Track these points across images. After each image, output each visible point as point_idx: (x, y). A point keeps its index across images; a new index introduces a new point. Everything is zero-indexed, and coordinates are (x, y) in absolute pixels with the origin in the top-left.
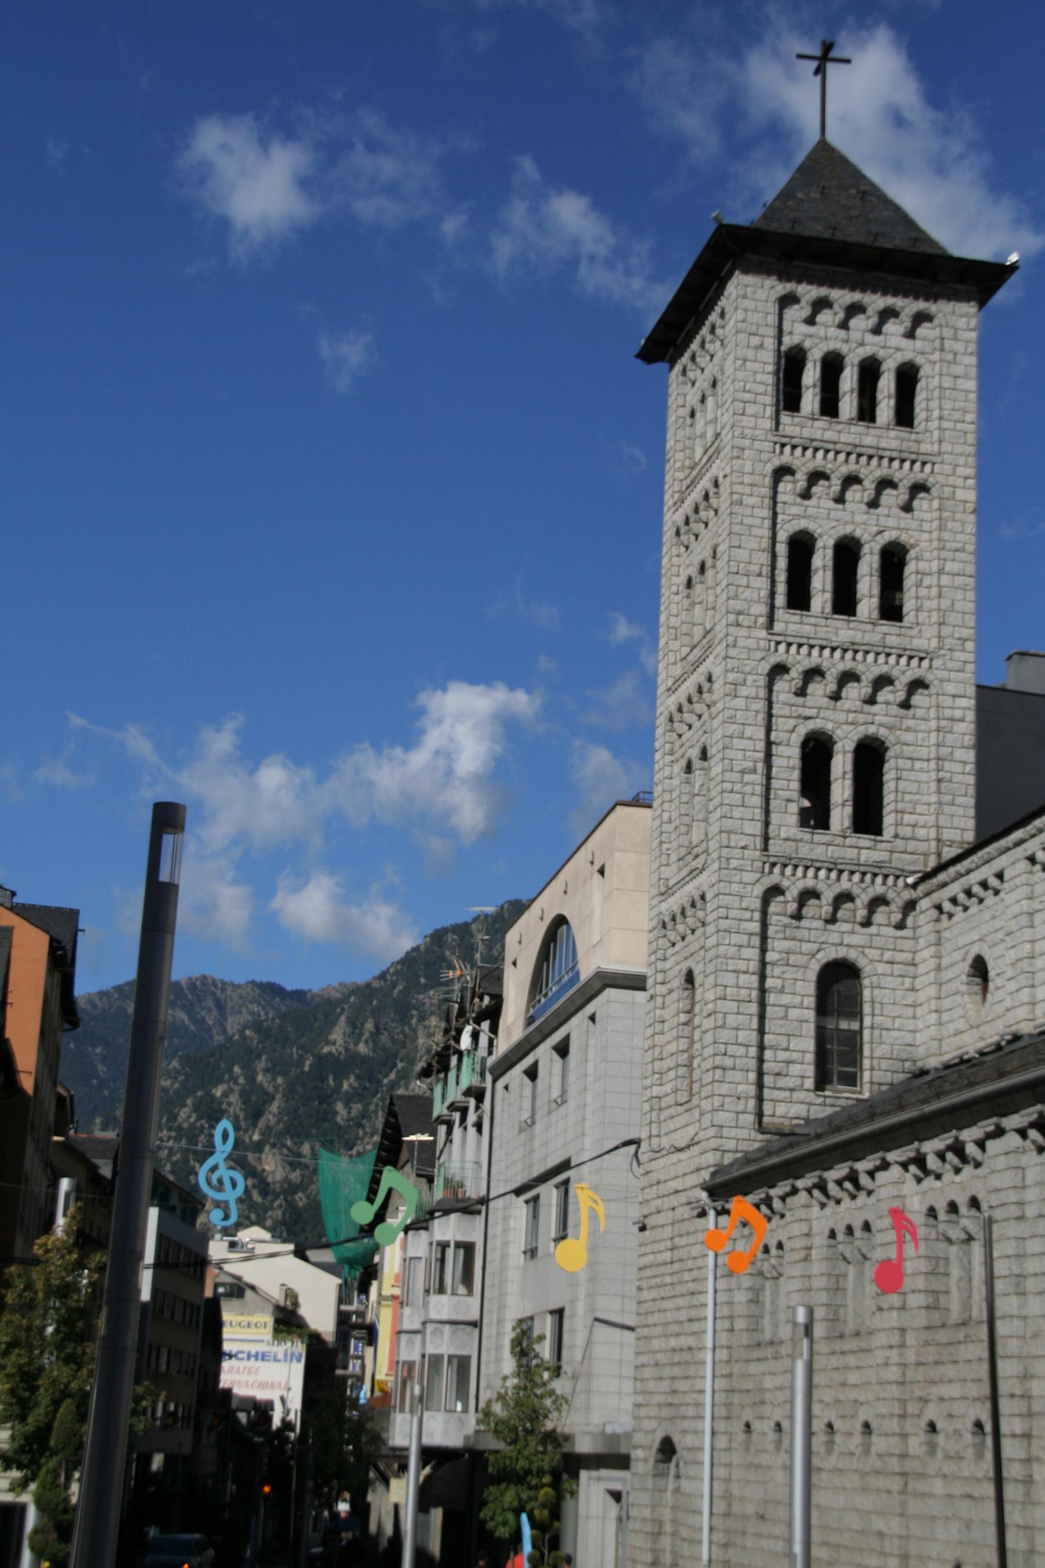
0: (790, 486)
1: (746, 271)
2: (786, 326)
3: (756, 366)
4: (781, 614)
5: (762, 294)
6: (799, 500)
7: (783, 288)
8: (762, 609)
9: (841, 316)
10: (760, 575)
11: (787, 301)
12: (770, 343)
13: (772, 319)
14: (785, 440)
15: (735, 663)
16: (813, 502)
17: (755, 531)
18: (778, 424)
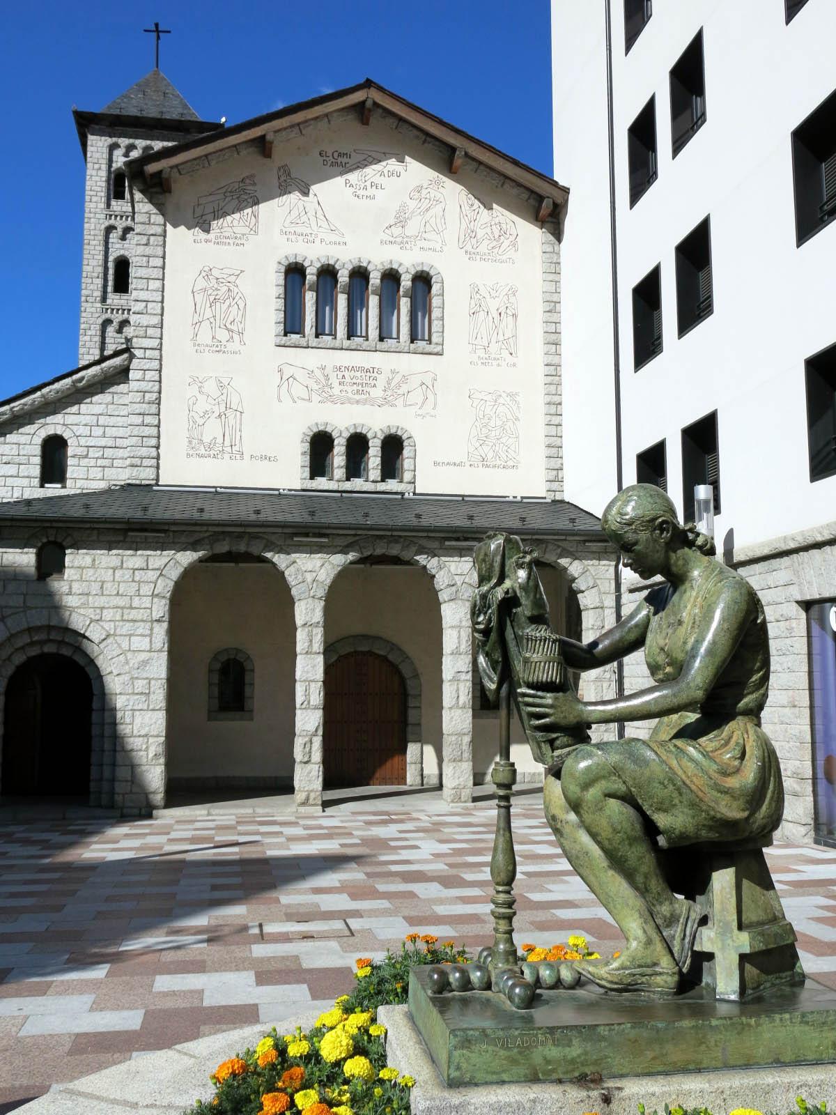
0: (115, 235)
1: (92, 134)
2: (115, 158)
3: (98, 179)
5: (100, 144)
6: (120, 241)
7: (110, 141)
8: (98, 294)
10: (98, 277)
11: (113, 147)
12: (104, 167)
13: (106, 156)
15: (85, 319)
16: (127, 241)
17: (95, 257)
18: (108, 205)
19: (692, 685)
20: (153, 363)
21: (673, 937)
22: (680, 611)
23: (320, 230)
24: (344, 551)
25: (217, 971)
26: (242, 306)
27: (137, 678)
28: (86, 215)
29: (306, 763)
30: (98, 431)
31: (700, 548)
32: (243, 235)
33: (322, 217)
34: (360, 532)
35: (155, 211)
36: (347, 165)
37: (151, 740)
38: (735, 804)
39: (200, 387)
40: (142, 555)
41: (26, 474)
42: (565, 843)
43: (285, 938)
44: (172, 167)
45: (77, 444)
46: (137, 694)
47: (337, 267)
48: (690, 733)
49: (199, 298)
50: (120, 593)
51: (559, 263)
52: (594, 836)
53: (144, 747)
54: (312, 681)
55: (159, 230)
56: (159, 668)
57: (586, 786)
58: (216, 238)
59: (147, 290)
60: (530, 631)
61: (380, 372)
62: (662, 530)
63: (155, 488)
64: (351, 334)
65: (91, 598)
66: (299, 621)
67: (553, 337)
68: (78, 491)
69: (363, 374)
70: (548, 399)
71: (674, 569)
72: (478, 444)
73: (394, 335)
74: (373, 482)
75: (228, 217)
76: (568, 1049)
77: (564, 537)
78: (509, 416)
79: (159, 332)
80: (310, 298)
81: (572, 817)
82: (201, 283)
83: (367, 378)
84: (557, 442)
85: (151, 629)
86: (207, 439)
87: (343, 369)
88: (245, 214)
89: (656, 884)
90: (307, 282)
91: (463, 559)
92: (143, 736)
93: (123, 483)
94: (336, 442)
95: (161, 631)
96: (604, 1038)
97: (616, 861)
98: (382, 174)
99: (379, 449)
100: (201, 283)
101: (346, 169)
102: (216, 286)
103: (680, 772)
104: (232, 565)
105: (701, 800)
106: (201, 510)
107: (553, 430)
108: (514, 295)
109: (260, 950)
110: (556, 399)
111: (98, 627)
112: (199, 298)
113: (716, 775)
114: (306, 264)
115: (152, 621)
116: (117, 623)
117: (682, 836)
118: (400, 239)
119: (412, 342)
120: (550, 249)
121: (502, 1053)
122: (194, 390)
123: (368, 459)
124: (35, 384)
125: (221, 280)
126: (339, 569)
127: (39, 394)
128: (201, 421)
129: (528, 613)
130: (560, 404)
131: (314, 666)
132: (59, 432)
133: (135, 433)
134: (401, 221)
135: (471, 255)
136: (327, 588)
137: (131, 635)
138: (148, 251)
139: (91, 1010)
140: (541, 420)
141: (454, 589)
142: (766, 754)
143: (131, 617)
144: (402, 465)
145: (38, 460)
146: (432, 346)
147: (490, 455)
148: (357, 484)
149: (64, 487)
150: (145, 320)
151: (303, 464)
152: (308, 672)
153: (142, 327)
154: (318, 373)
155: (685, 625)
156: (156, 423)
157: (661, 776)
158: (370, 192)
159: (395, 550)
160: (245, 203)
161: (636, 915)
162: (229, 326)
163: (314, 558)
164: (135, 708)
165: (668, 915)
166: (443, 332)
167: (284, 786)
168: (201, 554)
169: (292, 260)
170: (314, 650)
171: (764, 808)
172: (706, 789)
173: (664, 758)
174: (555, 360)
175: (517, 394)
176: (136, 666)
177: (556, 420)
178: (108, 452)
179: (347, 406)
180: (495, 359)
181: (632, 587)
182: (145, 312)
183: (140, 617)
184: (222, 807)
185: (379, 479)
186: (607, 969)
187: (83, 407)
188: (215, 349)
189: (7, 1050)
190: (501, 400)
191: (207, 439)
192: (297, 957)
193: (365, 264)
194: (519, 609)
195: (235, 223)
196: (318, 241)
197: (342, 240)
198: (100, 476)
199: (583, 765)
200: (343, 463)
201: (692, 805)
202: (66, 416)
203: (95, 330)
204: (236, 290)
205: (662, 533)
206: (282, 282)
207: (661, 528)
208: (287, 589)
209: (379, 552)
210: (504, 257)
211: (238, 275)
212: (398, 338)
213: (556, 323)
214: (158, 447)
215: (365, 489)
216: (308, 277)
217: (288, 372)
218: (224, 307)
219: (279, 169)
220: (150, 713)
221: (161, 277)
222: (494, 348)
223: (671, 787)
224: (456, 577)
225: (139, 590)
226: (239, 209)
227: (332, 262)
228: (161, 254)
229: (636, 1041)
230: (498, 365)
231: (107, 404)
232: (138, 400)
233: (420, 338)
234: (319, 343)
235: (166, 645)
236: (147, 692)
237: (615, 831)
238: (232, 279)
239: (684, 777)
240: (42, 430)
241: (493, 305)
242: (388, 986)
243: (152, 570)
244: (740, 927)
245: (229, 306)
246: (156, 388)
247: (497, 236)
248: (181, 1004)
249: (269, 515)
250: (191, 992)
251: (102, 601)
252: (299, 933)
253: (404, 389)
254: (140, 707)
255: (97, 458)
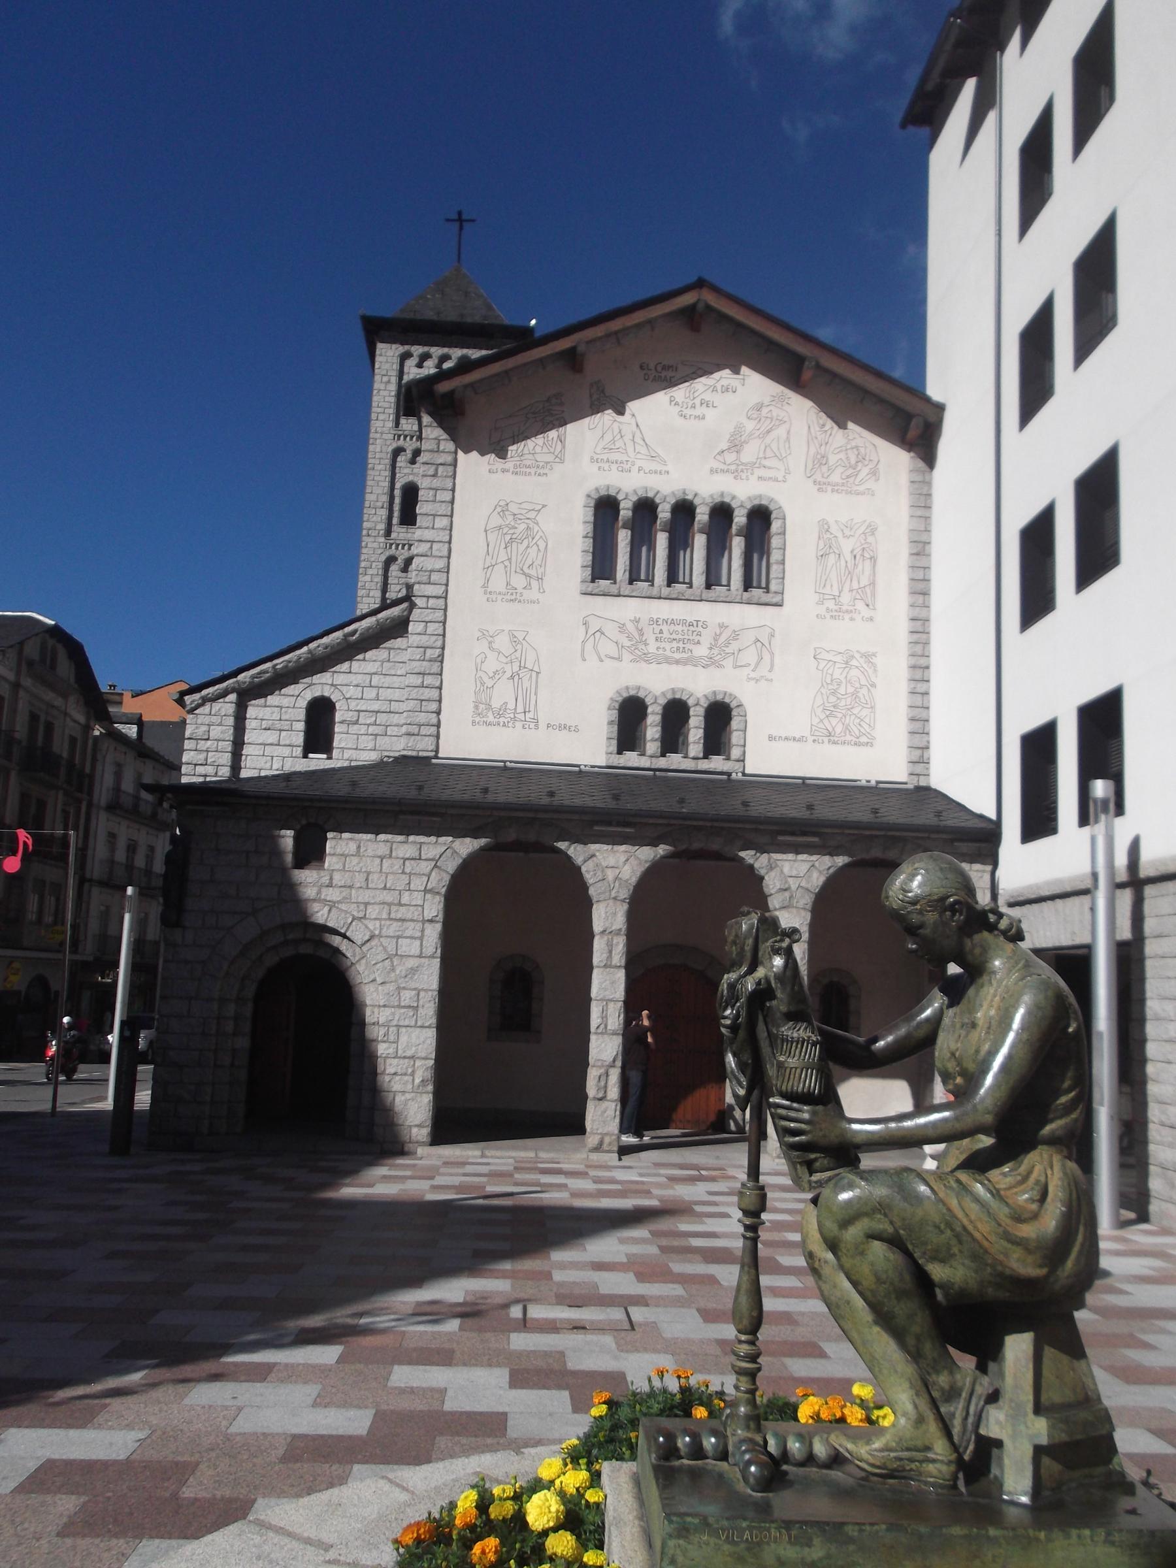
0: (404, 458)
2: (406, 369)
3: (386, 393)
4: (395, 528)
5: (390, 353)
6: (409, 465)
7: (401, 349)
8: (382, 526)
9: (436, 361)
10: (382, 507)
11: (405, 357)
12: (394, 380)
13: (396, 366)
14: (400, 432)
15: (366, 556)
17: (381, 484)
18: (397, 424)
19: (979, 1107)
20: (437, 614)
21: (953, 1415)
22: (972, 1011)
23: (639, 456)
24: (654, 843)
25: (465, 1365)
26: (542, 545)
27: (404, 988)
28: (371, 435)
29: (600, 1099)
30: (372, 693)
31: (1004, 933)
32: (547, 463)
33: (642, 442)
34: (673, 822)
35: (445, 436)
36: (673, 380)
37: (418, 1063)
38: (1030, 1259)
39: (490, 643)
40: (415, 842)
41: (288, 742)
42: (825, 1287)
43: (551, 1327)
44: (466, 386)
45: (346, 708)
46: (404, 1007)
47: (657, 500)
48: (978, 1163)
49: (492, 537)
50: (388, 886)
51: (930, 495)
52: (855, 1284)
53: (410, 1070)
54: (611, 1000)
55: (449, 458)
56: (430, 977)
57: (845, 1224)
58: (515, 466)
59: (433, 528)
60: (788, 1030)
61: (705, 626)
62: (954, 912)
63: (434, 761)
64: (672, 579)
65: (353, 891)
66: (597, 925)
67: (921, 586)
68: (346, 764)
69: (684, 628)
70: (913, 661)
71: (969, 958)
72: (822, 716)
73: (724, 582)
74: (695, 758)
75: (529, 441)
76: (807, 1550)
77: (926, 835)
78: (864, 682)
79: (445, 578)
80: (623, 538)
81: (830, 1256)
82: (496, 521)
83: (690, 633)
84: (922, 714)
85: (423, 931)
86: (496, 704)
87: (660, 622)
88: (550, 438)
89: (928, 1347)
90: (620, 518)
91: (800, 857)
92: (409, 1058)
93: (397, 754)
94: (650, 710)
95: (433, 933)
96: (851, 1540)
97: (884, 1318)
98: (714, 390)
99: (702, 719)
100: (496, 521)
101: (670, 383)
102: (512, 523)
103: (960, 1215)
104: (521, 854)
105: (986, 1251)
106: (486, 791)
107: (918, 700)
108: (873, 534)
109: (520, 1341)
110: (922, 662)
111: (360, 924)
112: (492, 537)
113: (1008, 1221)
114: (620, 497)
115: (424, 921)
116: (383, 922)
117: (963, 1293)
118: (733, 467)
119: (746, 590)
120: (919, 478)
121: (726, 1547)
122: (485, 643)
123: (689, 730)
124: (301, 638)
125: (519, 516)
126: (647, 865)
127: (305, 649)
128: (489, 683)
129: (784, 1008)
130: (927, 667)
131: (613, 983)
132: (326, 694)
133: (413, 696)
134: (736, 445)
135: (821, 487)
136: (632, 888)
137: (398, 937)
138: (436, 483)
139: (315, 1405)
140: (903, 687)
141: (787, 894)
142: (1074, 1196)
143: (399, 916)
144: (730, 740)
145: (301, 726)
146: (770, 595)
147: (839, 729)
148: (674, 761)
149: (330, 758)
150: (429, 564)
151: (610, 736)
152: (605, 989)
153: (426, 571)
154: (630, 627)
155: (979, 1029)
156: (438, 684)
157: (937, 1220)
158: (699, 411)
159: (715, 845)
160: (551, 426)
161: (906, 1385)
162: (526, 571)
163: (617, 851)
164: (401, 1023)
165: (947, 1387)
166: (783, 578)
167: (574, 1125)
168: (483, 842)
169: (603, 493)
170: (613, 963)
171: (1069, 1264)
172: (993, 1238)
173: (941, 1195)
174: (923, 615)
175: (874, 655)
176: (403, 973)
177: (921, 687)
178: (382, 718)
179: (665, 666)
180: (847, 611)
181: (1012, 900)
182: (429, 554)
183: (409, 916)
184: (497, 1149)
185: (701, 755)
186: (868, 1448)
187: (355, 665)
188: (509, 597)
189: (212, 1450)
190: (854, 662)
191: (496, 704)
192: (562, 1354)
193: (690, 497)
194: (774, 1003)
195: (538, 449)
196: (635, 469)
197: (664, 468)
198: (371, 745)
199: (845, 1196)
200: (657, 736)
201: (975, 1257)
202: (335, 675)
203: (377, 568)
204: (536, 528)
205: (954, 915)
206: (591, 519)
207: (952, 908)
208: (583, 887)
209: (696, 846)
210: (861, 488)
211: (539, 511)
212: (729, 585)
213: (925, 568)
214: (438, 713)
215: (683, 767)
216: (622, 513)
217: (595, 625)
218: (522, 547)
219: (591, 385)
220: (418, 1029)
221: (449, 514)
222: (846, 598)
223: (949, 1233)
224: (791, 880)
225: (409, 883)
226: (543, 430)
227: (650, 495)
228: (450, 485)
229: (892, 1547)
230: (852, 619)
231: (383, 662)
232: (418, 657)
233: (755, 585)
234: (633, 591)
235: (439, 951)
236: (415, 1005)
237: (879, 1280)
238: (532, 515)
239: (965, 1221)
240: (308, 691)
241: (847, 546)
242: (621, 1434)
243: (426, 860)
244: (1038, 1410)
245: (528, 547)
246: (439, 644)
247: (853, 461)
248: (419, 1405)
249: (566, 797)
250: (432, 1390)
251: (365, 896)
252: (568, 1321)
253: (734, 646)
254: (406, 1023)
255: (369, 725)
